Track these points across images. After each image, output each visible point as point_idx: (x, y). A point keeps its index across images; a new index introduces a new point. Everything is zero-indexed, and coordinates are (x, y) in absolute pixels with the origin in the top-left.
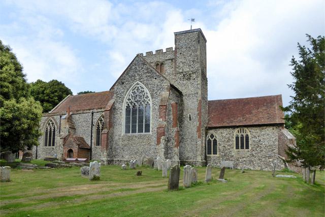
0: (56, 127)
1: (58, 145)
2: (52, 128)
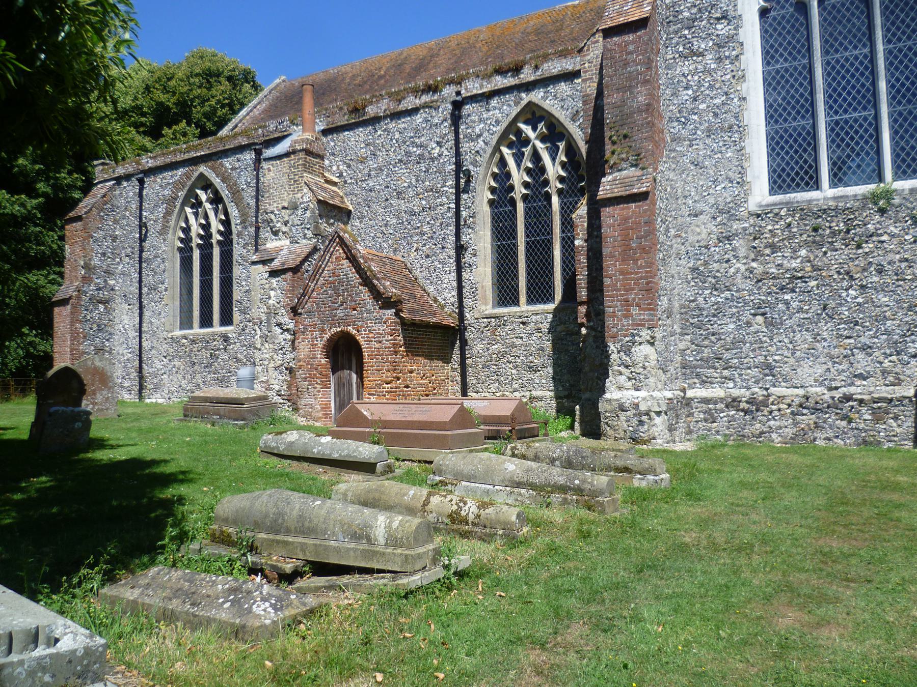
0: (234, 212)
1: (258, 312)
2: (216, 226)
